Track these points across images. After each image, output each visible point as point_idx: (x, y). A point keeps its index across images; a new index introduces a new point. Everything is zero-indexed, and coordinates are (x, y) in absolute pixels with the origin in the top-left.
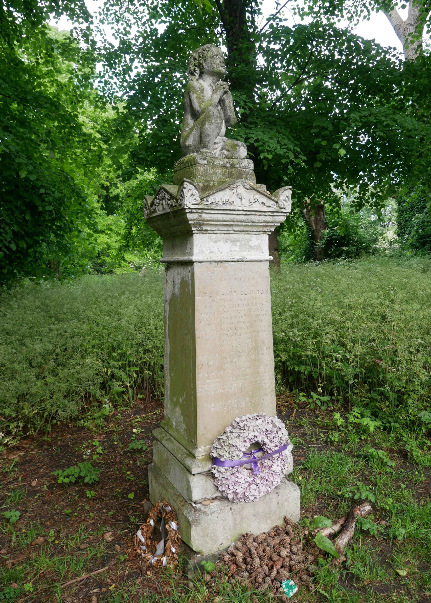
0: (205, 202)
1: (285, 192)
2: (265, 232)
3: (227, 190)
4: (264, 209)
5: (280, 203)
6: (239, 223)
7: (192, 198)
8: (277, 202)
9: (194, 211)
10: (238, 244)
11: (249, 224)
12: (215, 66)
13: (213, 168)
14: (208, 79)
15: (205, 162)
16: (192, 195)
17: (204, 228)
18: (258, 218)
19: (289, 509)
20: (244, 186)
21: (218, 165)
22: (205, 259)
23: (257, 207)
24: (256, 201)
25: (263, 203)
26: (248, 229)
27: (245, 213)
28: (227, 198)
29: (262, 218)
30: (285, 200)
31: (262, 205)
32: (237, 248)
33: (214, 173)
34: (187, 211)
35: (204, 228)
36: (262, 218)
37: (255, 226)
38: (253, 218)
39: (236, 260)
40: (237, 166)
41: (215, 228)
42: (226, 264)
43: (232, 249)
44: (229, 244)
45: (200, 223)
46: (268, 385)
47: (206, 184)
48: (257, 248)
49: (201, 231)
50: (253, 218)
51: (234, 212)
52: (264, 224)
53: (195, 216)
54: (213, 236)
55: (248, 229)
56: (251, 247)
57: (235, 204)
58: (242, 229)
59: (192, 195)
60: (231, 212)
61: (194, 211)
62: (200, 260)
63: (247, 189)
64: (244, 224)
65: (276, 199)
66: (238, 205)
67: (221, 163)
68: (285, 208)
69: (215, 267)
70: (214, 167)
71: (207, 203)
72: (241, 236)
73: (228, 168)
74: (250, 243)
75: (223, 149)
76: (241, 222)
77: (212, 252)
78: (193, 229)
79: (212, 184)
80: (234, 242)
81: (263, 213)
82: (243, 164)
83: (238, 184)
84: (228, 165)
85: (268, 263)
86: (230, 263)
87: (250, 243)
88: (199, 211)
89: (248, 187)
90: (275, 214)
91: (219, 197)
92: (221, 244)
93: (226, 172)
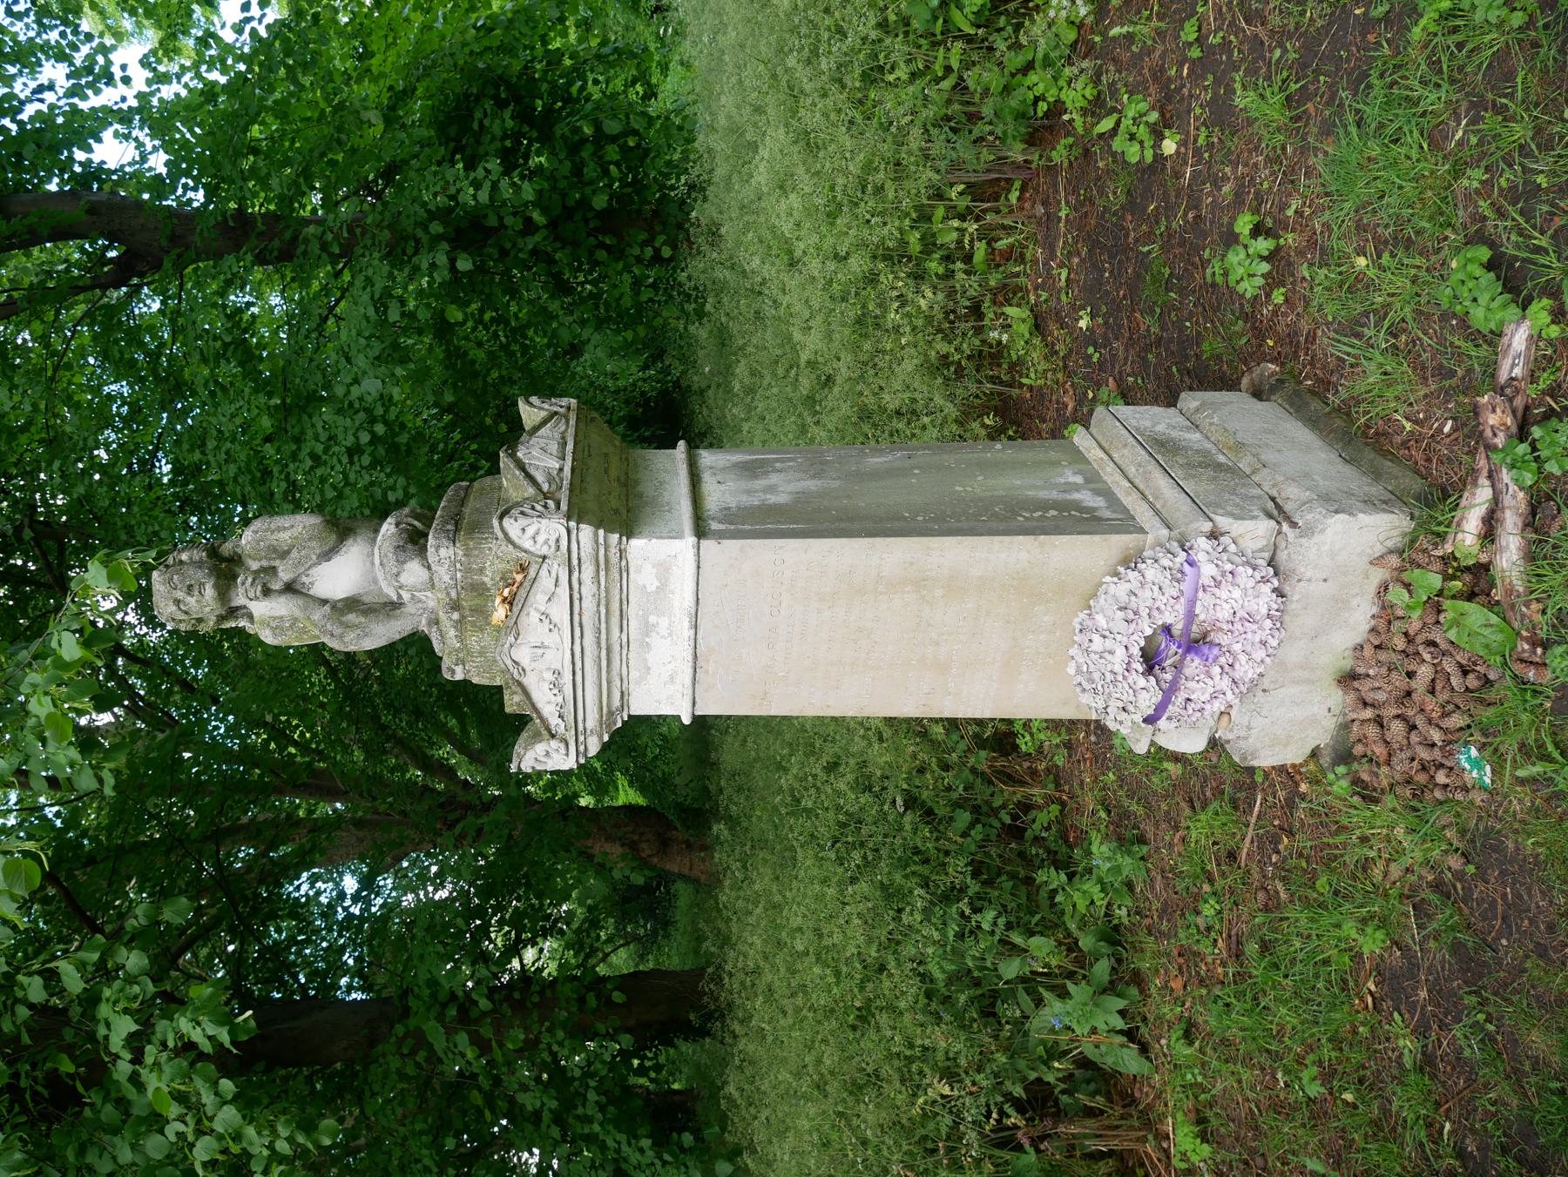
0: (562, 730)
2: (622, 553)
3: (525, 681)
4: (563, 591)
6: (603, 636)
7: (554, 755)
8: (544, 558)
9: (582, 748)
10: (652, 619)
16: (547, 754)
18: (589, 604)
19: (1359, 550)
21: (460, 638)
23: (560, 612)
26: (615, 606)
28: (546, 686)
29: (588, 589)
31: (555, 599)
33: (481, 654)
34: (582, 761)
35: (616, 703)
36: (588, 589)
40: (453, 594)
43: (665, 632)
44: (653, 640)
48: (664, 570)
51: (578, 665)
52: (602, 573)
54: (634, 674)
55: (615, 606)
56: (663, 588)
60: (579, 673)
61: (582, 748)
66: (558, 654)
67: (452, 633)
69: (707, 672)
70: (465, 647)
72: (633, 611)
73: (463, 617)
77: (672, 678)
78: (619, 724)
80: (648, 629)
81: (576, 596)
82: (446, 578)
83: (509, 662)
84: (456, 616)
86: (700, 640)
88: (581, 738)
90: (575, 562)
92: (652, 658)
93: (473, 624)
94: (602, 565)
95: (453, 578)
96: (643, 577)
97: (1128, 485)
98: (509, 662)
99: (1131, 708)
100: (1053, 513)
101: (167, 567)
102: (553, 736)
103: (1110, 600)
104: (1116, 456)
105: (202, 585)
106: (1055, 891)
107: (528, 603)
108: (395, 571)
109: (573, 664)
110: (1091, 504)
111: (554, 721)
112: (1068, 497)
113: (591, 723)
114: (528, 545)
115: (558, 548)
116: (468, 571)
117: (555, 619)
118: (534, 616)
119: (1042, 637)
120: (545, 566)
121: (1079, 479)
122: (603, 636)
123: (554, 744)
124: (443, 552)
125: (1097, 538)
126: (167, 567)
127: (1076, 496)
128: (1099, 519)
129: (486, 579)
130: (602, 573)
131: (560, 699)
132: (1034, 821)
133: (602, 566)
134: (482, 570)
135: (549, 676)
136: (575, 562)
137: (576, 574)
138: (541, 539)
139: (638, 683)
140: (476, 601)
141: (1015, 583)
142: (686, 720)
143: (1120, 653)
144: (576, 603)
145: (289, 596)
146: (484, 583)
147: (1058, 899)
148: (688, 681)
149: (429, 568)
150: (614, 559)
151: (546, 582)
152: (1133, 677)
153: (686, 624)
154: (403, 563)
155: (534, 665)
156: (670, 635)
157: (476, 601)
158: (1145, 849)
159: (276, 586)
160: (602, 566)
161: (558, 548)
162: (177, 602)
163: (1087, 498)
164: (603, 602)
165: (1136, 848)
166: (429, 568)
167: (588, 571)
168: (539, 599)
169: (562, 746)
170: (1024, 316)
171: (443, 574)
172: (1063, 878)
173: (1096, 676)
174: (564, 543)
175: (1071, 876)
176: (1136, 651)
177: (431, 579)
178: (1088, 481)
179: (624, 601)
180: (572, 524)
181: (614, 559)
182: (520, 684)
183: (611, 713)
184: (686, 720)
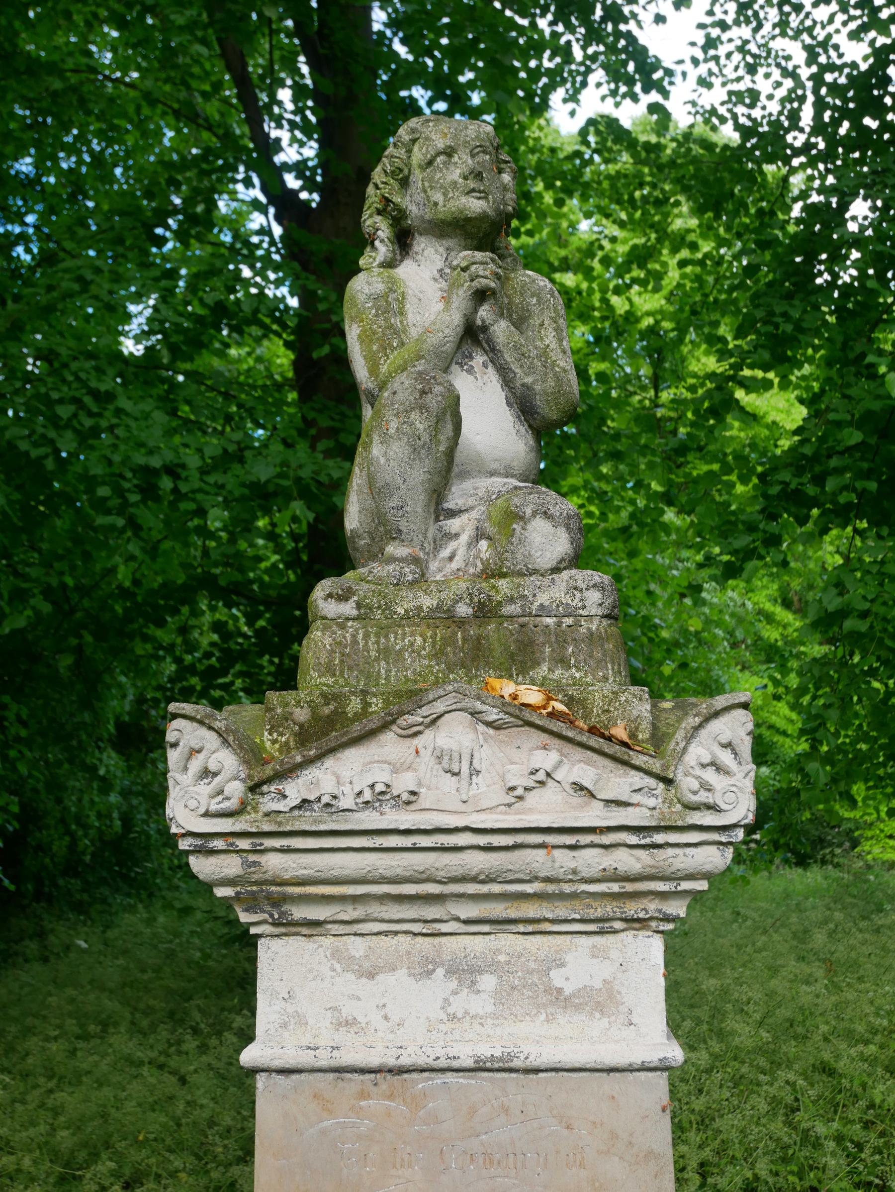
0: (269, 804)
1: (717, 726)
2: (637, 923)
3: (389, 737)
4: (593, 815)
5: (687, 783)
6: (471, 888)
7: (204, 789)
8: (668, 782)
9: (219, 844)
10: (488, 982)
11: (529, 888)
12: (438, 197)
13: (383, 630)
14: (430, 252)
15: (348, 608)
16: (207, 773)
17: (299, 912)
18: (564, 861)
20: (474, 714)
21: (415, 616)
22: (306, 1059)
23: (548, 808)
24: (543, 780)
25: (579, 788)
26: (531, 910)
27: (482, 840)
28: (381, 776)
29: (591, 861)
30: (718, 768)
31: (578, 799)
32: (481, 1004)
33: (385, 652)
35: (299, 912)
36: (591, 861)
37: (562, 896)
38: (536, 860)
39: (469, 1063)
40: (510, 609)
41: (350, 913)
42: (421, 1082)
43: (458, 1005)
45: (274, 897)
47: (327, 710)
48: (600, 1001)
49: (288, 926)
50: (536, 860)
51: (425, 841)
52: (615, 887)
53: (231, 866)
54: (357, 947)
55: (531, 910)
56: (559, 999)
57: (425, 801)
58: (498, 910)
59: (207, 773)
60: (407, 841)
61: (219, 844)
62: (277, 1063)
63: (489, 724)
64: (496, 888)
65: (656, 766)
66: (445, 802)
68: (712, 807)
69: (363, 1095)
71: (281, 806)
72: (507, 943)
73: (462, 623)
75: (480, 534)
76: (474, 879)
77: (349, 1023)
78: (244, 917)
79: (354, 705)
80: (465, 973)
82: (543, 599)
83: (440, 707)
84: (463, 610)
85: (661, 1081)
87: (557, 978)
88: (244, 844)
89: (493, 715)
90: (659, 838)
91: (344, 775)
93: (449, 641)
94: (627, 887)
95: (543, 610)
96: (582, 961)
98: (440, 707)
101: (497, 148)
102: (255, 788)
105: (484, 195)
107: (569, 748)
108: (554, 511)
109: (407, 832)
111: (295, 790)
113: (274, 863)
114: (698, 752)
115: (695, 807)
116: (561, 638)
117: (532, 799)
118: (546, 759)
120: (652, 782)
122: (471, 888)
123: (236, 790)
124: (594, 596)
126: (497, 148)
129: (544, 668)
130: (615, 887)
131: (347, 802)
133: (630, 887)
134: (563, 661)
135: (403, 784)
136: (659, 838)
137: (633, 839)
138: (710, 775)
139: (336, 954)
140: (498, 649)
142: (249, 1056)
144: (570, 840)
145: (460, 330)
146: (536, 664)
148: (347, 1058)
149: (556, 570)
150: (632, 909)
151: (620, 783)
153: (485, 1050)
154: (567, 527)
155: (426, 755)
156: (453, 1018)
157: (498, 649)
159: (485, 312)
160: (630, 887)
161: (695, 807)
162: (449, 152)
164: (551, 888)
166: (556, 570)
167: (627, 861)
168: (583, 769)
169: (232, 804)
171: (552, 593)
174: (708, 819)
177: (535, 572)
179: (534, 926)
180: (740, 834)
181: (632, 909)
182: (385, 726)
183: (277, 902)
184: (249, 1056)
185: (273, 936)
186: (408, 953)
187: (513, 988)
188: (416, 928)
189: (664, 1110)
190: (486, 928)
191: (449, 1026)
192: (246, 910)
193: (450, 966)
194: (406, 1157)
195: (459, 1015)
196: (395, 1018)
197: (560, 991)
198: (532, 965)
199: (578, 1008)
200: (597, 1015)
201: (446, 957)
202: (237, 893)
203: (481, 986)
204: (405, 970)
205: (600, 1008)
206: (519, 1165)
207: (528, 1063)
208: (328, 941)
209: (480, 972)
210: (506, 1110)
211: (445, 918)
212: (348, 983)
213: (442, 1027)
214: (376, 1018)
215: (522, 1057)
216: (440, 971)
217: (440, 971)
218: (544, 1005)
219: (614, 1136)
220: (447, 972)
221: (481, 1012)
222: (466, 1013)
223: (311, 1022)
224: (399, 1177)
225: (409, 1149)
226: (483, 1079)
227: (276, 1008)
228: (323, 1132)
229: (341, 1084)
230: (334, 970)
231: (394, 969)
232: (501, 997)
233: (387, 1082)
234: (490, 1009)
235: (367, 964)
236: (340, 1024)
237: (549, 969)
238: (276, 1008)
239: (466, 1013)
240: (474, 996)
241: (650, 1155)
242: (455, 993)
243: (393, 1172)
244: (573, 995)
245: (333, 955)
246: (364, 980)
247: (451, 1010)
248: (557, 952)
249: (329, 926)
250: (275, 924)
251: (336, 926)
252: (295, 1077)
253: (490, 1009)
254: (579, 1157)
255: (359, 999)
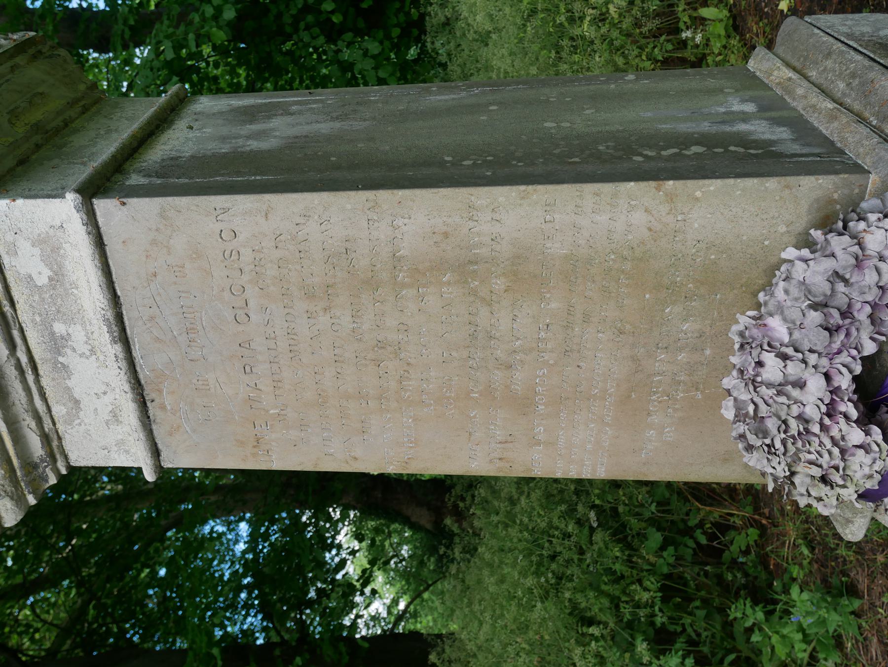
10: (59, 328)
32: (78, 335)
39: (118, 348)
46: (639, 218)
54: (58, 410)
56: (57, 278)
69: (163, 407)
74: (42, 280)
78: (53, 480)
80: (58, 344)
87: (42, 280)
97: (830, 105)
99: (836, 478)
100: (696, 149)
103: (795, 292)
104: (813, 74)
106: (750, 631)
110: (767, 136)
112: (727, 128)
119: (682, 357)
121: (750, 108)
125: (772, 183)
127: (743, 127)
128: (780, 155)
132: (732, 543)
139: (69, 422)
141: (628, 266)
142: (150, 476)
143: (816, 386)
147: (756, 638)
152: (839, 428)
156: (93, 351)
158: (856, 604)
163: (760, 129)
165: (845, 601)
170: (721, 16)
172: (760, 616)
173: (772, 424)
175: (769, 614)
176: (844, 382)
178: (762, 109)
185: (66, 457)
186: (53, 379)
187: (58, 312)
188: (30, 378)
189: (124, 204)
190: (16, 333)
191: (99, 354)
192: (47, 481)
193: (55, 353)
194: (200, 382)
195: (90, 347)
196: (104, 388)
197: (51, 279)
198: (37, 298)
199: (60, 267)
200: (62, 251)
201: (49, 356)
202: (30, 493)
203: (64, 333)
204: (67, 381)
205: (56, 249)
206: (191, 310)
207: (107, 308)
208: (61, 428)
209: (53, 334)
210: (152, 318)
211: (13, 362)
212: (86, 415)
213: (102, 358)
214: (107, 399)
215: (103, 312)
216: (61, 359)
217: (61, 359)
218: (65, 290)
219: (154, 242)
220: (60, 355)
221: (83, 333)
222: (86, 343)
223: (120, 437)
224: (215, 387)
225: (195, 381)
226: (132, 333)
227: (116, 456)
228: (194, 431)
229: (158, 421)
230: (80, 424)
231: (68, 388)
232: (69, 320)
233: (149, 394)
234: (79, 327)
235: (70, 405)
236: (117, 420)
237: (36, 286)
238: (116, 456)
239: (86, 343)
240: (73, 338)
241: (162, 215)
242: (74, 350)
243: (212, 390)
244: (51, 269)
245: (69, 424)
246: (82, 406)
247: (88, 353)
248: (21, 280)
249: (46, 430)
250: (54, 460)
251: (46, 426)
252: (160, 446)
253: (79, 327)
254: (175, 269)
255: (96, 409)
